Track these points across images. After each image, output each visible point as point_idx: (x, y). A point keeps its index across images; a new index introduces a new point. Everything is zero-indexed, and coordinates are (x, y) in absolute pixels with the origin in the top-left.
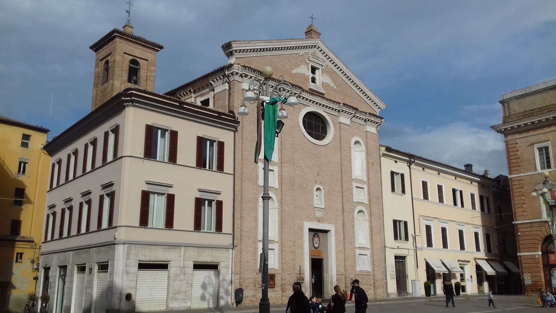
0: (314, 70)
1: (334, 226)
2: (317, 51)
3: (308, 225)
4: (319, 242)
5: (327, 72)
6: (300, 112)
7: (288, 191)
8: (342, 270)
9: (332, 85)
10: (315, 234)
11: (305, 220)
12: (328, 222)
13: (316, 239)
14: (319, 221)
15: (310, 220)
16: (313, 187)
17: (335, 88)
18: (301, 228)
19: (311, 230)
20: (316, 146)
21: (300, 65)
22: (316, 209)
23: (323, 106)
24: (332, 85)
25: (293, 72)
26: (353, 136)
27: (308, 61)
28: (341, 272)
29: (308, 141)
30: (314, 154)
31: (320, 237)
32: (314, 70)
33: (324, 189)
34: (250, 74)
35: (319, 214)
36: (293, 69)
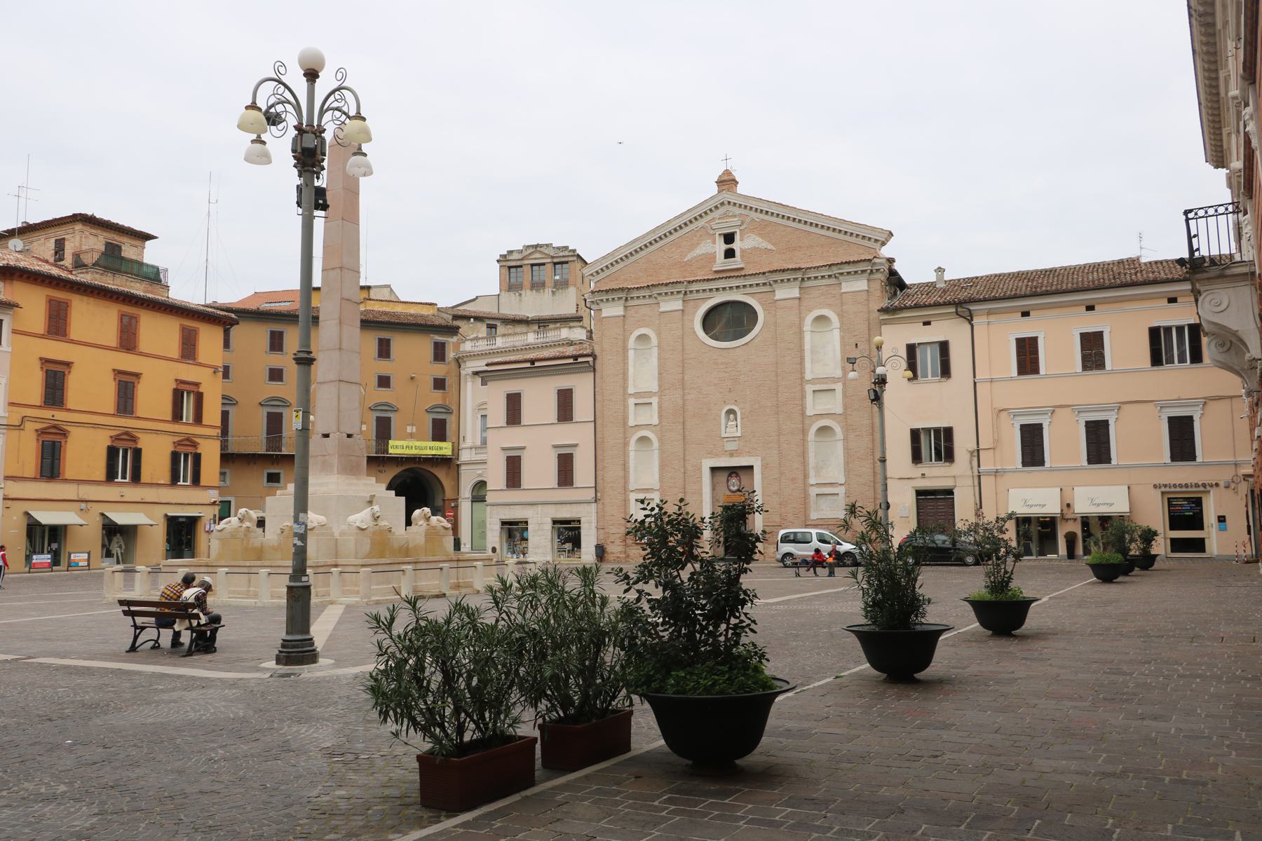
0: (729, 238)
1: (760, 458)
2: (731, 208)
3: (708, 464)
4: (740, 482)
5: (752, 231)
6: (696, 312)
7: (671, 424)
8: (778, 520)
9: (765, 245)
10: (730, 475)
11: (705, 458)
12: (750, 454)
13: (734, 480)
14: (731, 455)
15: (711, 454)
16: (721, 410)
17: (770, 247)
18: (699, 469)
19: (714, 470)
20: (726, 351)
21: (698, 244)
22: (725, 440)
23: (738, 287)
24: (765, 245)
25: (686, 259)
26: (810, 311)
27: (712, 232)
28: (775, 522)
29: (712, 349)
30: (722, 363)
31: (741, 477)
32: (729, 238)
33: (741, 409)
34: (604, 298)
35: (731, 446)
36: (686, 256)
